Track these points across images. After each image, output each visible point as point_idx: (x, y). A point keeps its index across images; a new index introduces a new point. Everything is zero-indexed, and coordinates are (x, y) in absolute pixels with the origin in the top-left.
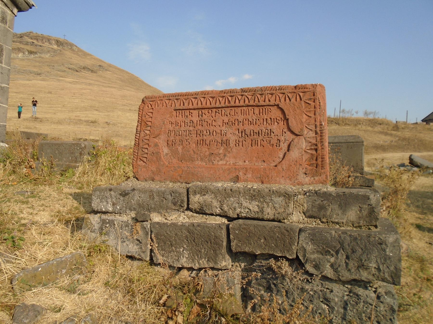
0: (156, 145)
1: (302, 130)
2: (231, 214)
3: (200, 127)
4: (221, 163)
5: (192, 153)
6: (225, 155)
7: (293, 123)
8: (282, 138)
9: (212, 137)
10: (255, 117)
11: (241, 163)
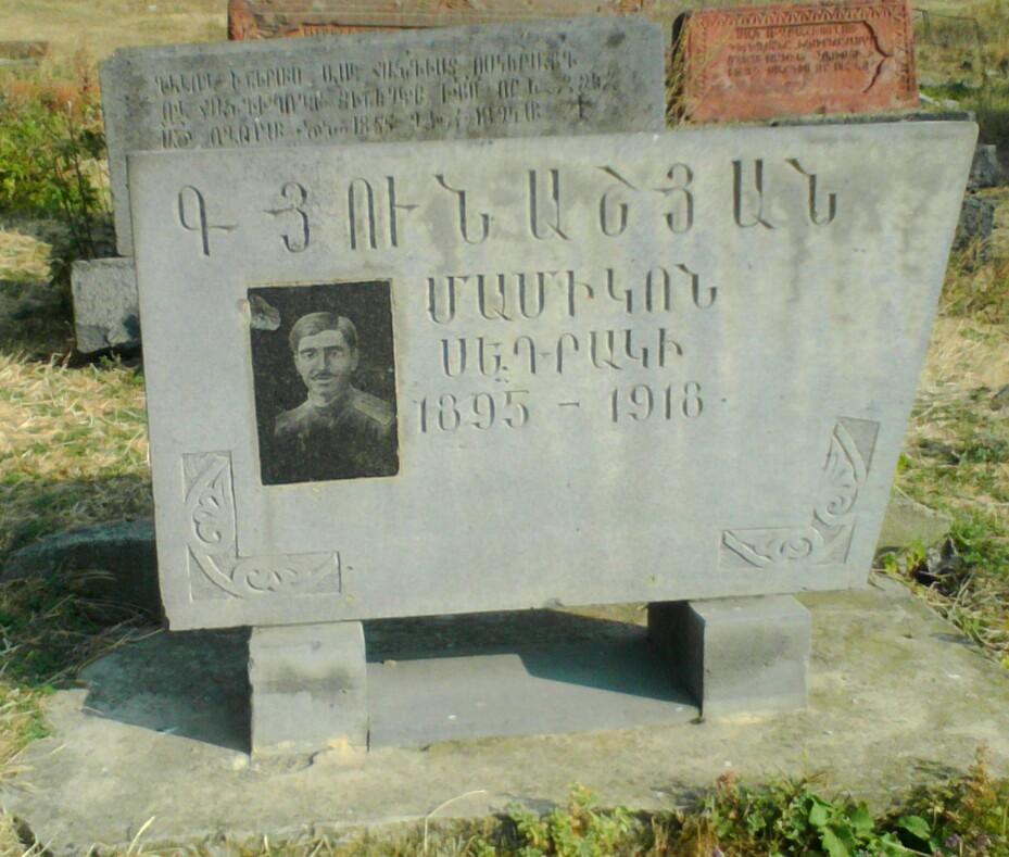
0: (716, 77)
4: (801, 93)
6: (805, 84)
7: (882, 41)
8: (870, 60)
9: (787, 63)
10: (837, 36)
11: (824, 92)
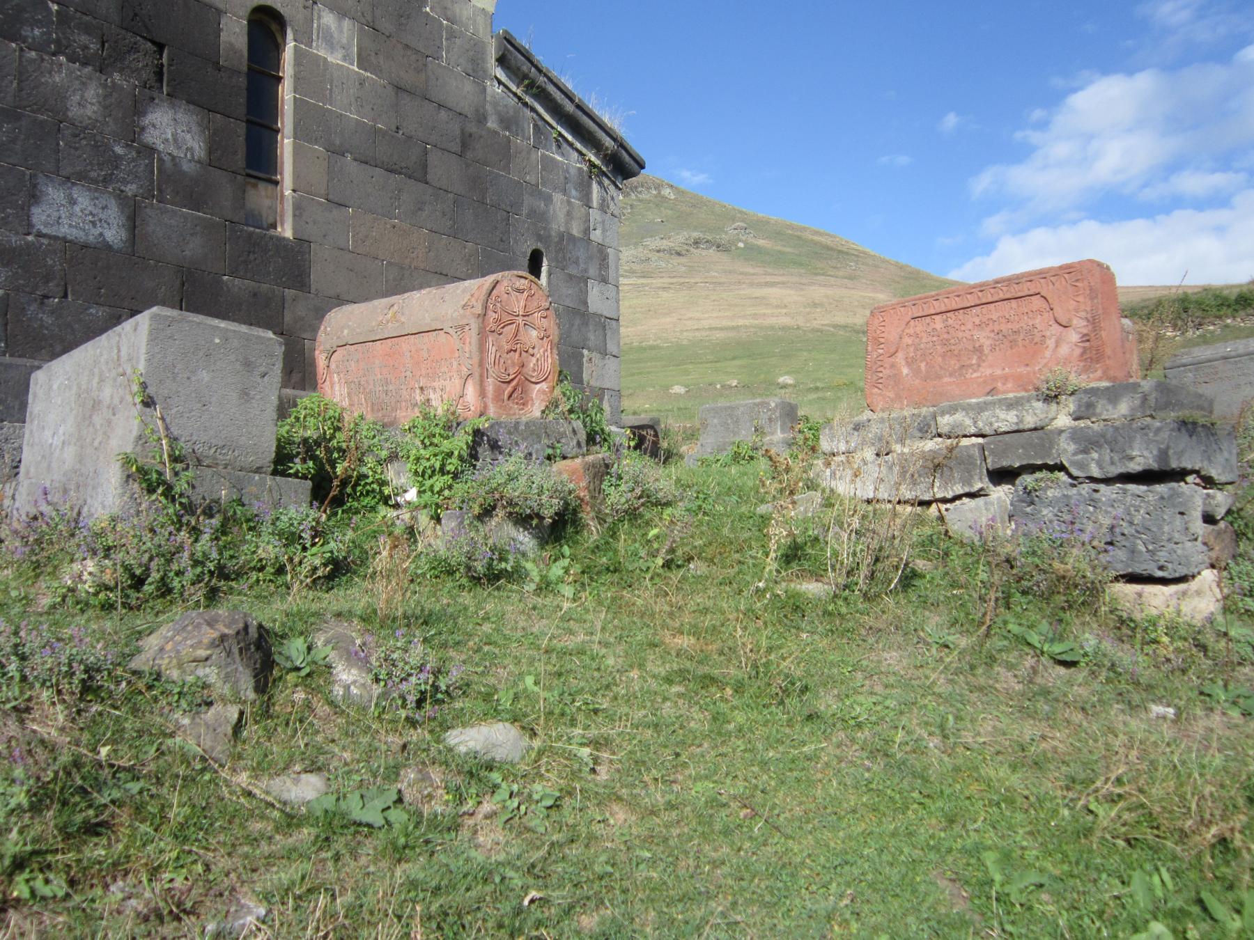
0: (893, 366)
1: (1070, 320)
2: (987, 430)
3: (946, 336)
4: (975, 375)
5: (938, 368)
8: (1048, 334)
11: (998, 372)
